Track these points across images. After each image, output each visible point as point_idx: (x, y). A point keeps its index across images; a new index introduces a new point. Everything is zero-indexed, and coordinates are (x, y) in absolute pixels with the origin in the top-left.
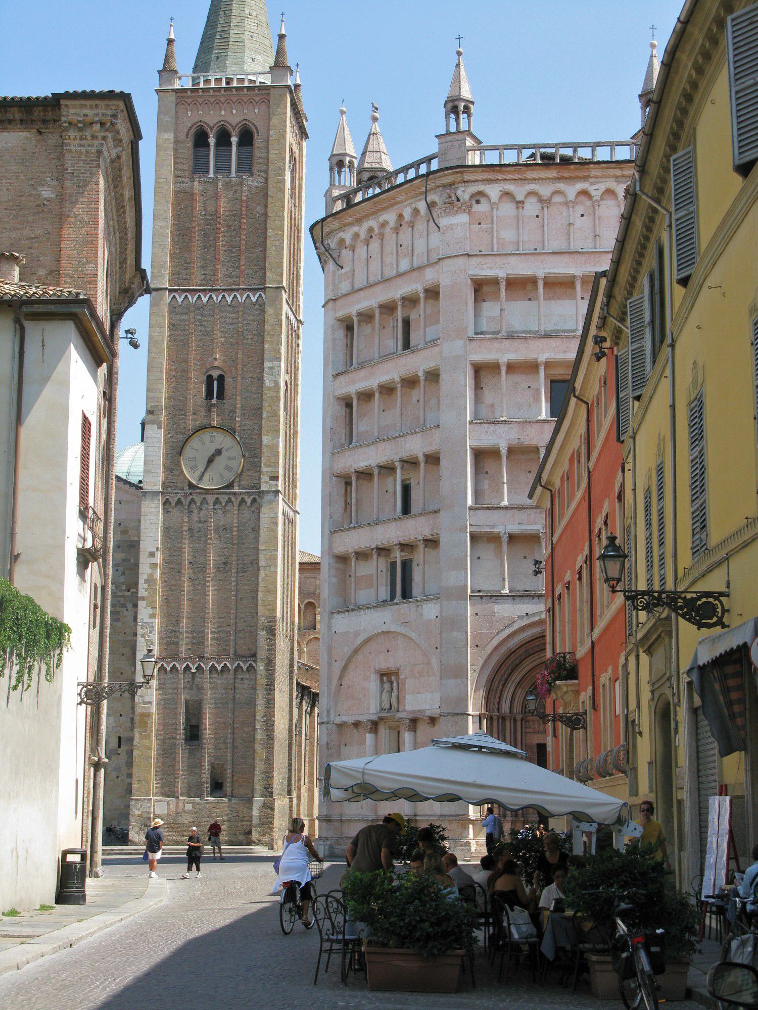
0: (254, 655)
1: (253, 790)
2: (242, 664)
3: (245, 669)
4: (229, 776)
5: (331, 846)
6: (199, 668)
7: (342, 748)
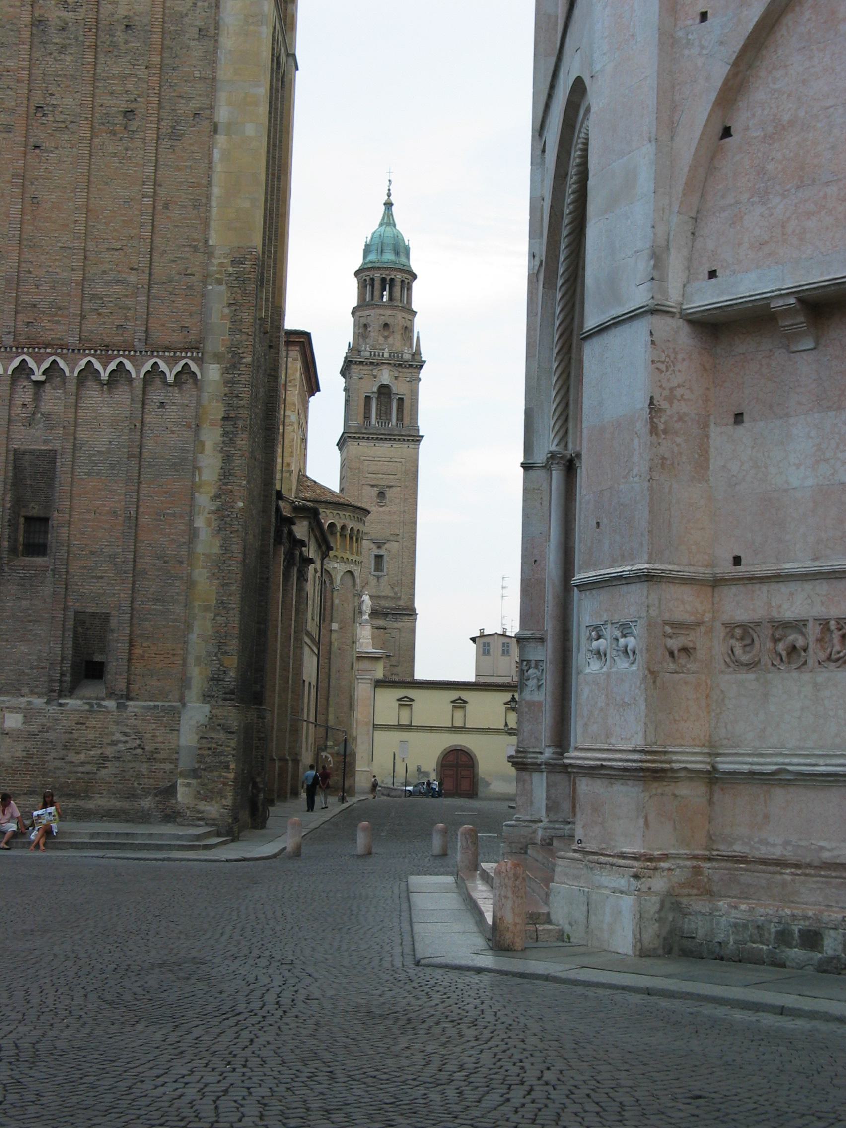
0: (195, 348)
1: (184, 682)
2: (163, 366)
3: (170, 378)
4: (123, 647)
5: (672, 903)
6: (52, 371)
7: (720, 437)
